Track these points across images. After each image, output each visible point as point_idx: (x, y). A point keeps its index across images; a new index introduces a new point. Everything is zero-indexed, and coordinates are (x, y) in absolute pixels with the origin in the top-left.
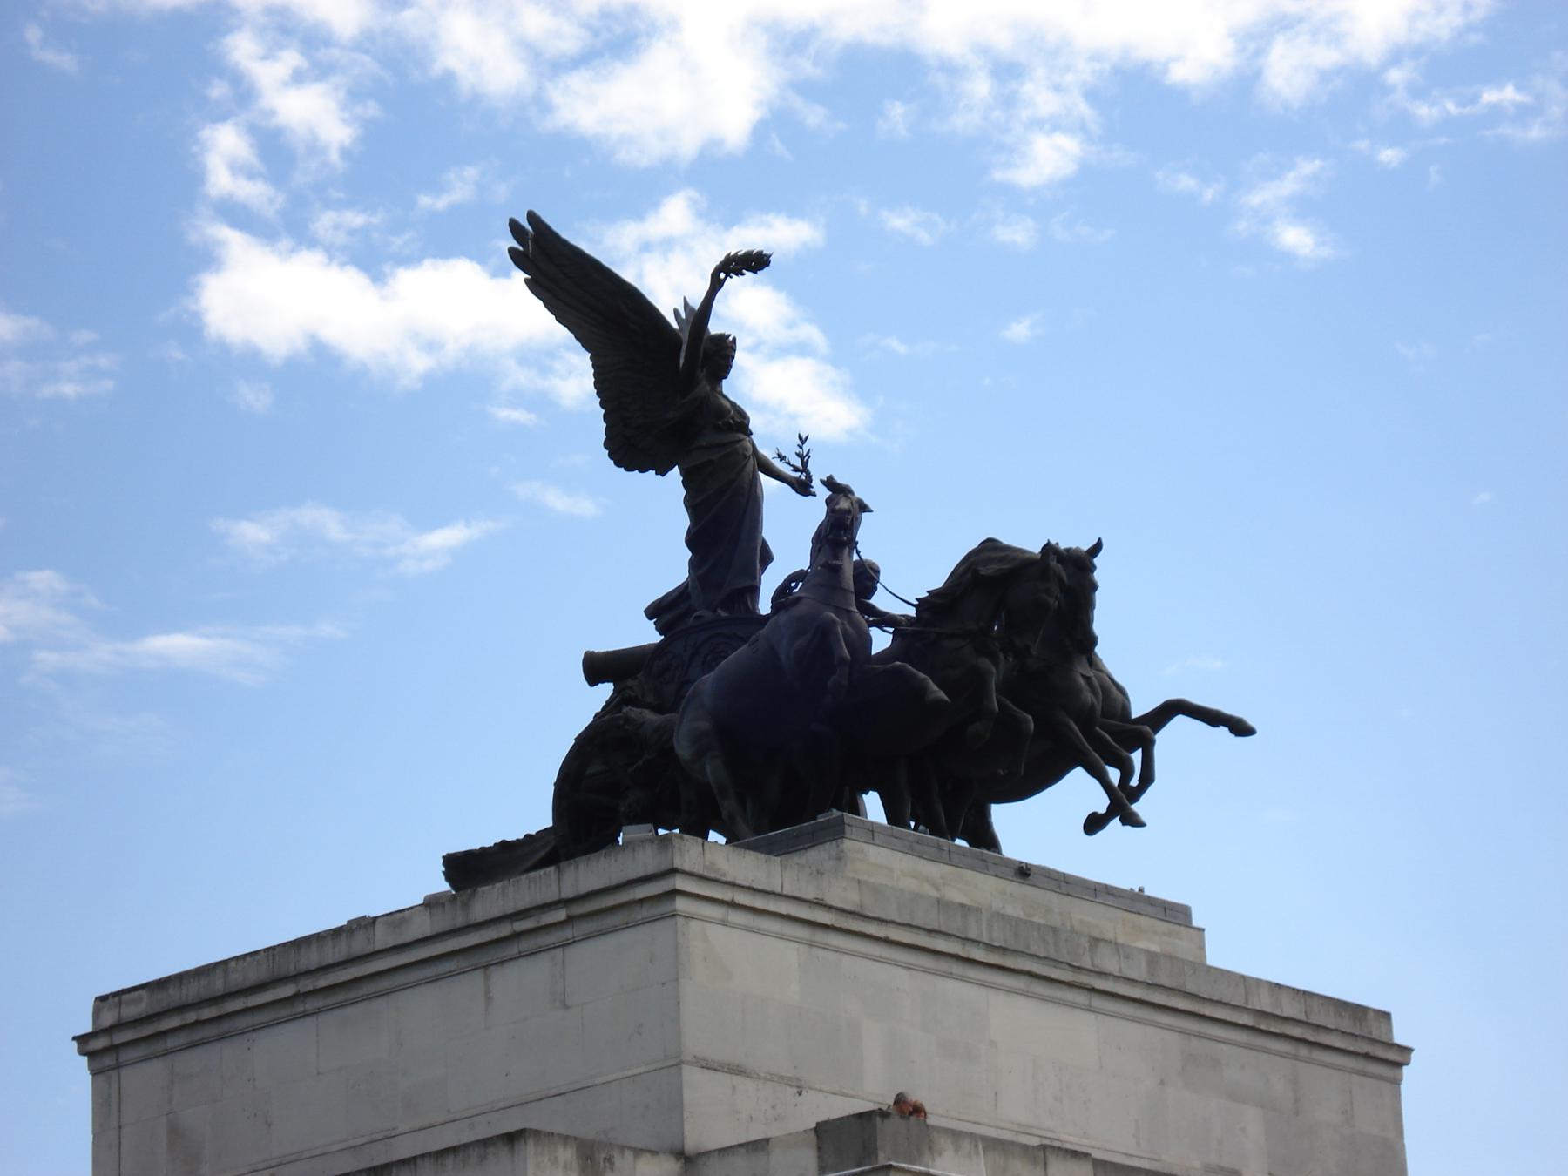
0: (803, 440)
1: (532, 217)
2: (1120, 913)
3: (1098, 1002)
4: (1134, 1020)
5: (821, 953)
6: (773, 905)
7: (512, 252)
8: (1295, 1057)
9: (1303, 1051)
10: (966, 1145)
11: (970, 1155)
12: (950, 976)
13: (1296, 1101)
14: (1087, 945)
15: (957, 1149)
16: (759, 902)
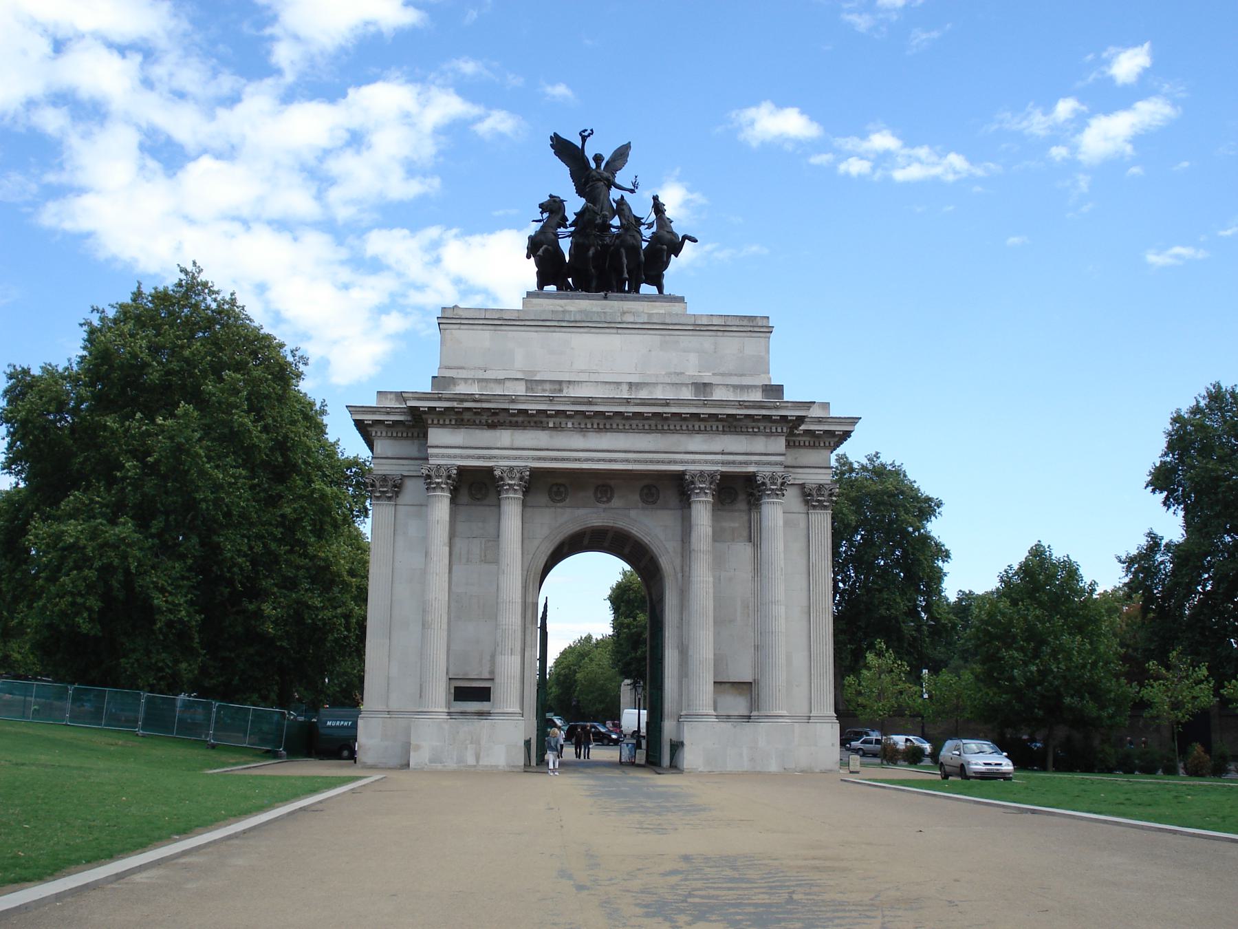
0: (636, 177)
1: (555, 134)
2: (649, 303)
3: (620, 331)
4: (638, 334)
5: (499, 332)
6: (476, 322)
7: (551, 145)
8: (716, 336)
9: (720, 333)
10: (470, 381)
11: (471, 384)
12: (555, 332)
13: (715, 349)
14: (619, 315)
15: (466, 383)
16: (471, 322)
